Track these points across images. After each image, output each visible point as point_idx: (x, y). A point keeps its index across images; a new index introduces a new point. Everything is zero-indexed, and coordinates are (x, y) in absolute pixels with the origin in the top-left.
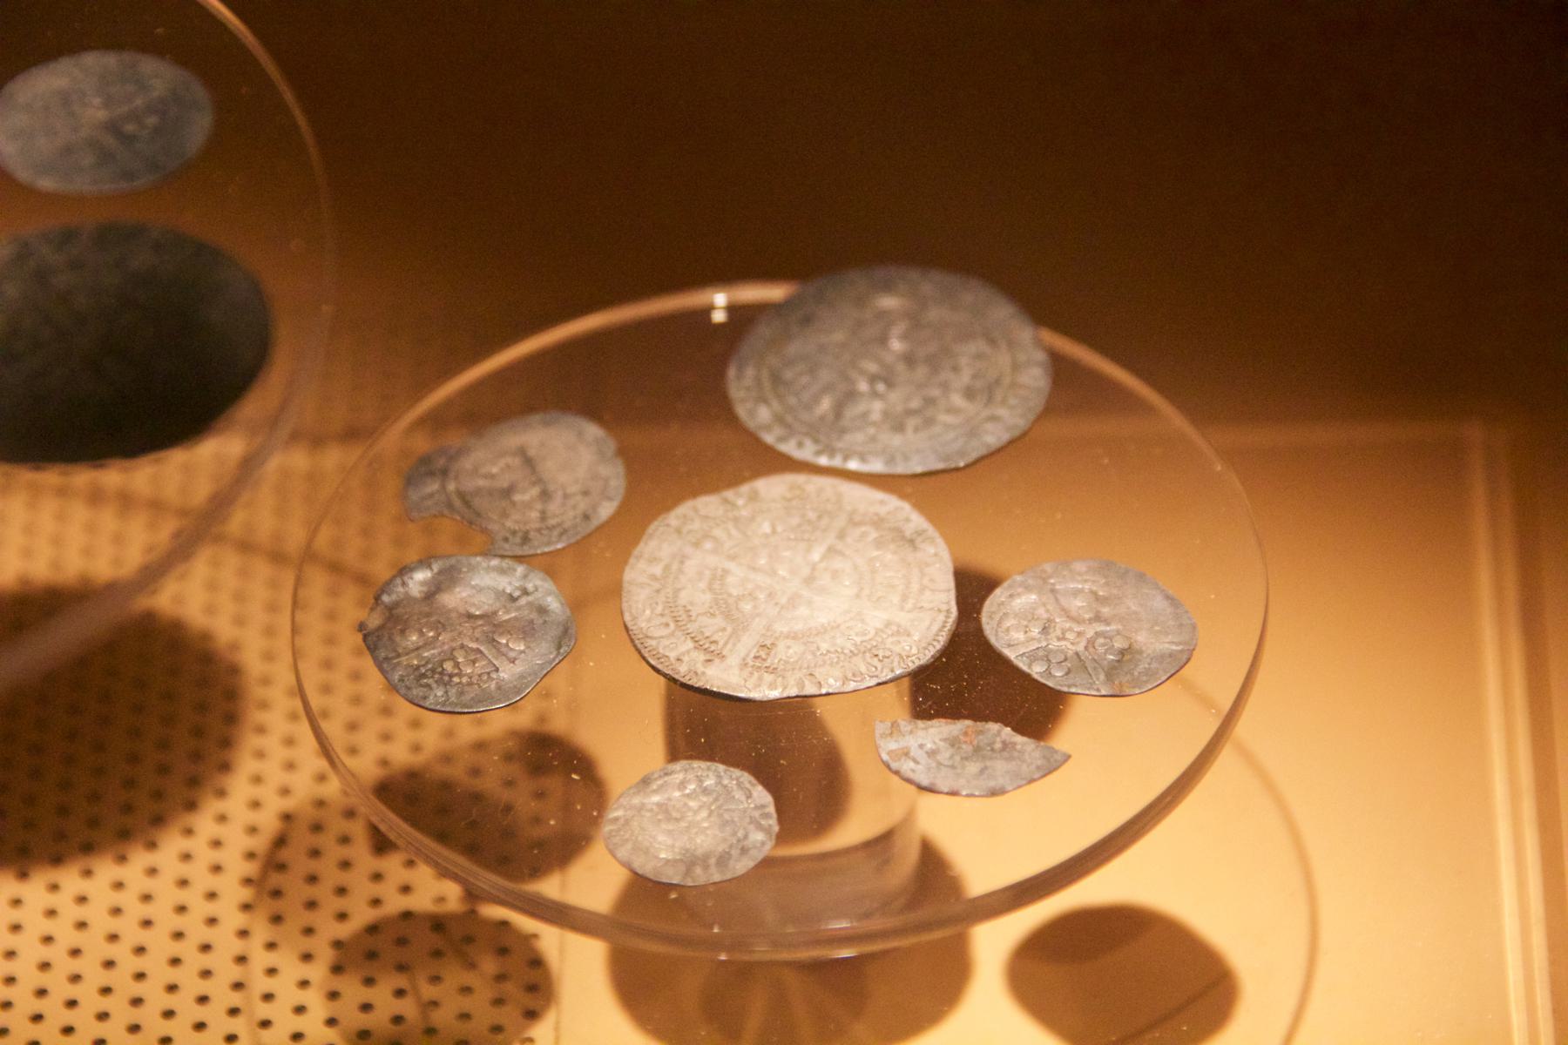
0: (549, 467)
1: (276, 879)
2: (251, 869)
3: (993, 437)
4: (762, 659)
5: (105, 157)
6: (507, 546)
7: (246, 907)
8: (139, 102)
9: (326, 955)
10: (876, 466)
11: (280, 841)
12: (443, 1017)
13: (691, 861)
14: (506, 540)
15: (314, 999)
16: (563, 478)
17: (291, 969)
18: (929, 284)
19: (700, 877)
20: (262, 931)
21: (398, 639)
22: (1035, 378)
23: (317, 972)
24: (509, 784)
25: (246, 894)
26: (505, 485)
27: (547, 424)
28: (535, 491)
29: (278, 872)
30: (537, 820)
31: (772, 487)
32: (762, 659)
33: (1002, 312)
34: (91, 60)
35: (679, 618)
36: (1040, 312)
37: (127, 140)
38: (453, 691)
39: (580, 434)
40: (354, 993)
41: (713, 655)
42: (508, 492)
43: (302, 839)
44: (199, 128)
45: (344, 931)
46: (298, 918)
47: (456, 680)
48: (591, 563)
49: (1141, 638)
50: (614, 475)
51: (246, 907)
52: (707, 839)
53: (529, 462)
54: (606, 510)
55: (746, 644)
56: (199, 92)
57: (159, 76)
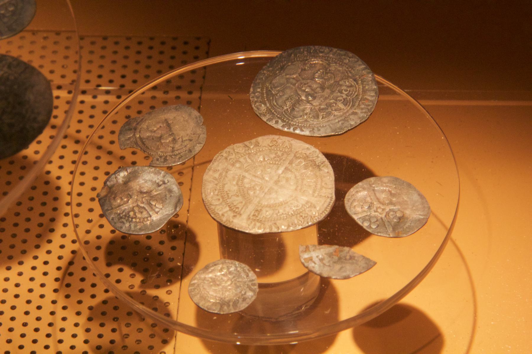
0: (176, 128)
2: (59, 274)
3: (353, 121)
4: (255, 217)
6: (158, 162)
7: (55, 291)
9: (86, 313)
10: (307, 133)
11: (71, 263)
12: (130, 342)
13: (223, 303)
14: (157, 160)
16: (182, 133)
17: (72, 319)
18: (333, 53)
19: (226, 310)
21: (112, 201)
22: (371, 96)
23: (82, 320)
25: (56, 285)
26: (159, 136)
27: (176, 110)
28: (170, 139)
29: (68, 277)
30: (171, 260)
31: (265, 141)
32: (255, 217)
33: (360, 67)
35: (224, 196)
36: (375, 69)
39: (190, 115)
40: (96, 329)
41: (237, 213)
45: (94, 302)
46: (76, 296)
47: (134, 220)
48: (190, 170)
49: (408, 212)
50: (202, 133)
51: (55, 291)
52: (230, 294)
53: (169, 125)
54: (198, 148)
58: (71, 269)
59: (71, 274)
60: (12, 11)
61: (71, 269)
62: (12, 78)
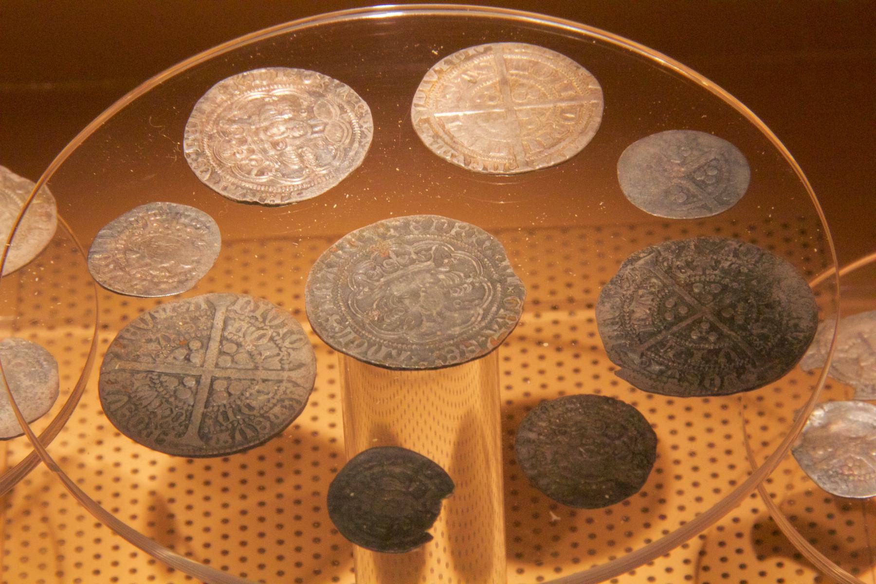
2: (689, 570)
5: (690, 197)
6: (864, 394)
8: (703, 161)
11: (702, 553)
14: (863, 390)
21: (812, 453)
24: (830, 516)
26: (855, 356)
30: (851, 539)
37: (701, 185)
38: (851, 485)
42: (857, 361)
44: (742, 178)
47: (851, 478)
53: (865, 341)
56: (737, 155)
57: (711, 145)
58: (706, 561)
59: (706, 569)
60: (715, 176)
61: (706, 561)
62: (745, 270)
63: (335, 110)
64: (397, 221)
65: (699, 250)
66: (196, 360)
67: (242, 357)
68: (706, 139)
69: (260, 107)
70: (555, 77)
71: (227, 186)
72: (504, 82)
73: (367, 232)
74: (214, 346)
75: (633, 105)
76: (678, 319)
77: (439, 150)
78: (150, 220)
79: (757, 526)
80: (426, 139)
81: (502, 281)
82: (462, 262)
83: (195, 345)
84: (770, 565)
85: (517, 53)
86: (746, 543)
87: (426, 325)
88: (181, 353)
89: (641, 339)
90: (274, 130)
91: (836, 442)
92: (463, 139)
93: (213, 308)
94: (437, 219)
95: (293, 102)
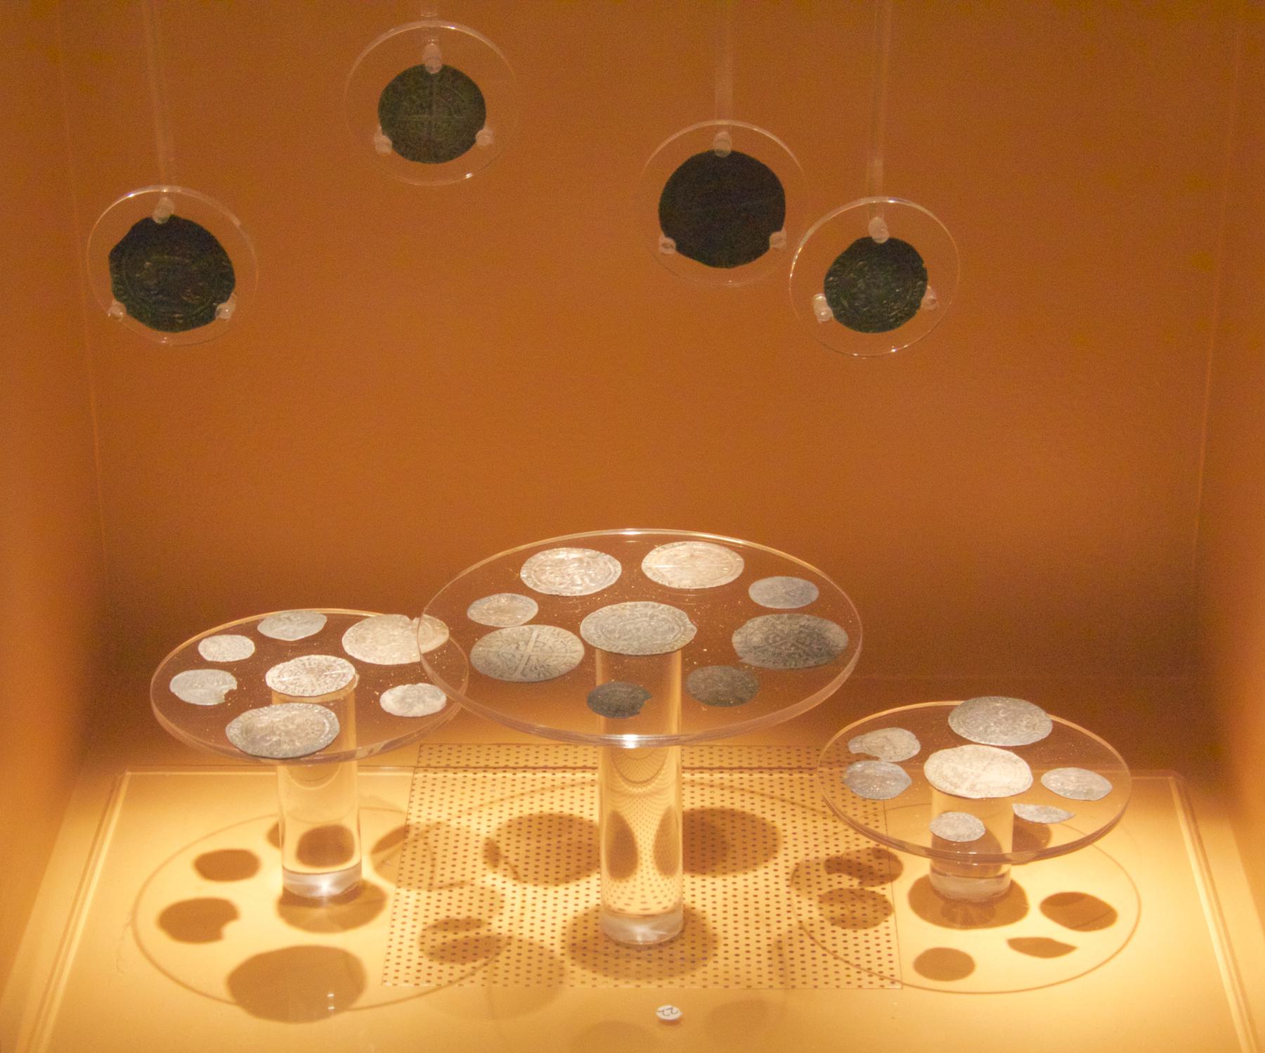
1: (796, 880)
4: (973, 787)
10: (1000, 744)
11: (796, 870)
15: (814, 909)
18: (1009, 700)
20: (794, 892)
23: (815, 902)
29: (797, 877)
31: (967, 748)
32: (973, 787)
33: (1034, 707)
34: (777, 578)
35: (945, 778)
41: (956, 786)
43: (803, 871)
45: (821, 893)
49: (1094, 787)
55: (967, 785)
56: (812, 585)
57: (801, 582)
63: (602, 564)
64: (632, 603)
65: (789, 618)
66: (522, 648)
67: (546, 648)
68: (796, 580)
69: (562, 561)
70: (719, 555)
71: (542, 589)
72: (692, 556)
73: (615, 607)
74: (531, 644)
75: (756, 567)
76: (775, 642)
77: (655, 579)
78: (503, 600)
79: (828, 861)
80: (649, 575)
81: (684, 625)
82: (664, 619)
83: (521, 643)
84: (834, 877)
85: (700, 546)
86: (821, 867)
87: (643, 640)
88: (514, 646)
89: (755, 648)
90: (570, 569)
91: (868, 777)
92: (669, 575)
93: (532, 630)
94: (651, 603)
95: (580, 560)
